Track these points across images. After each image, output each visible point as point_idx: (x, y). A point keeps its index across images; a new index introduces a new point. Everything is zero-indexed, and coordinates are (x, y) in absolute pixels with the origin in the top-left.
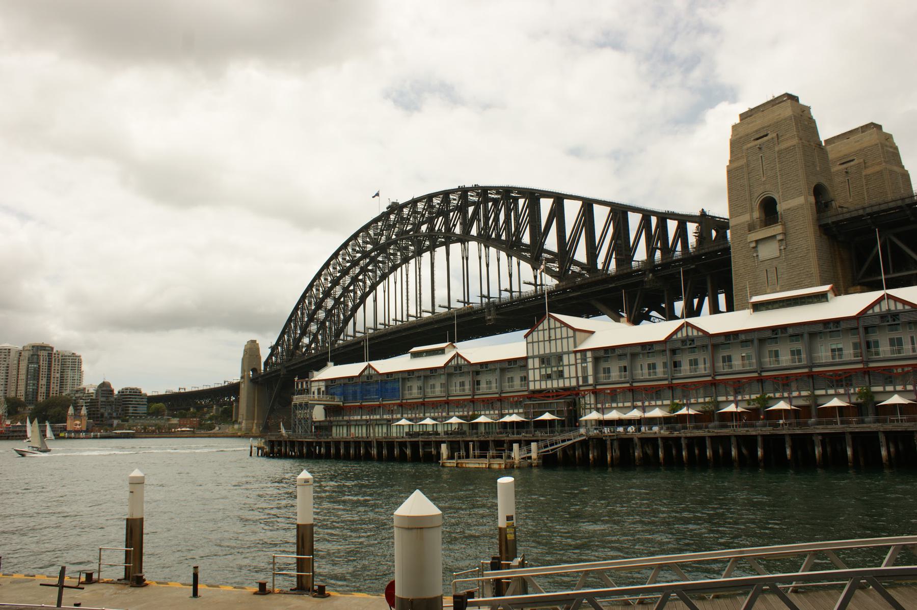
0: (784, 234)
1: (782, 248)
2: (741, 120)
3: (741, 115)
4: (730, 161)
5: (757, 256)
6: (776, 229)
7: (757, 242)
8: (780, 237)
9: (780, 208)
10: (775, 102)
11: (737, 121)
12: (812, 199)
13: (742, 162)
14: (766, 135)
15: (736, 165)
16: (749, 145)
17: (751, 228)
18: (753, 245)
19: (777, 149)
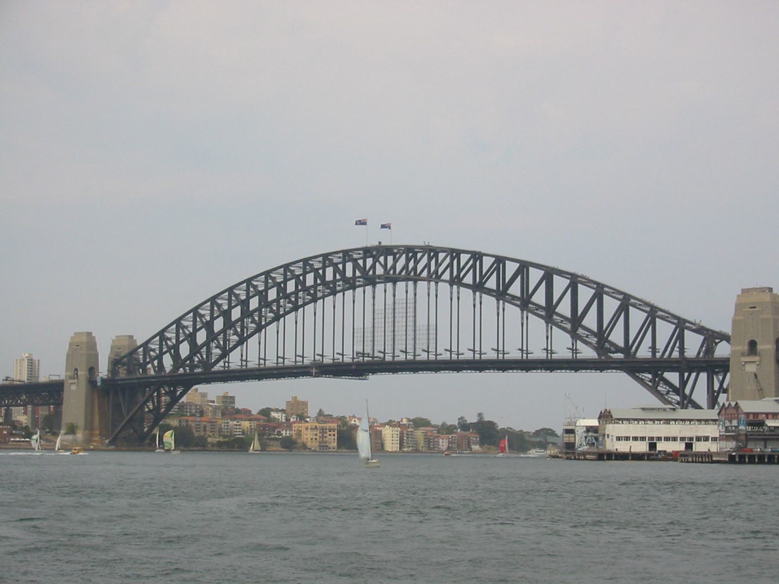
0: (760, 361)
1: (758, 368)
2: (742, 293)
3: (742, 290)
4: (735, 315)
5: (745, 369)
6: (756, 358)
7: (746, 362)
8: (758, 363)
9: (760, 347)
10: (762, 290)
11: (740, 293)
12: (775, 347)
13: (741, 318)
14: (755, 307)
15: (737, 318)
16: (746, 310)
17: (743, 355)
18: (743, 363)
19: (761, 317)
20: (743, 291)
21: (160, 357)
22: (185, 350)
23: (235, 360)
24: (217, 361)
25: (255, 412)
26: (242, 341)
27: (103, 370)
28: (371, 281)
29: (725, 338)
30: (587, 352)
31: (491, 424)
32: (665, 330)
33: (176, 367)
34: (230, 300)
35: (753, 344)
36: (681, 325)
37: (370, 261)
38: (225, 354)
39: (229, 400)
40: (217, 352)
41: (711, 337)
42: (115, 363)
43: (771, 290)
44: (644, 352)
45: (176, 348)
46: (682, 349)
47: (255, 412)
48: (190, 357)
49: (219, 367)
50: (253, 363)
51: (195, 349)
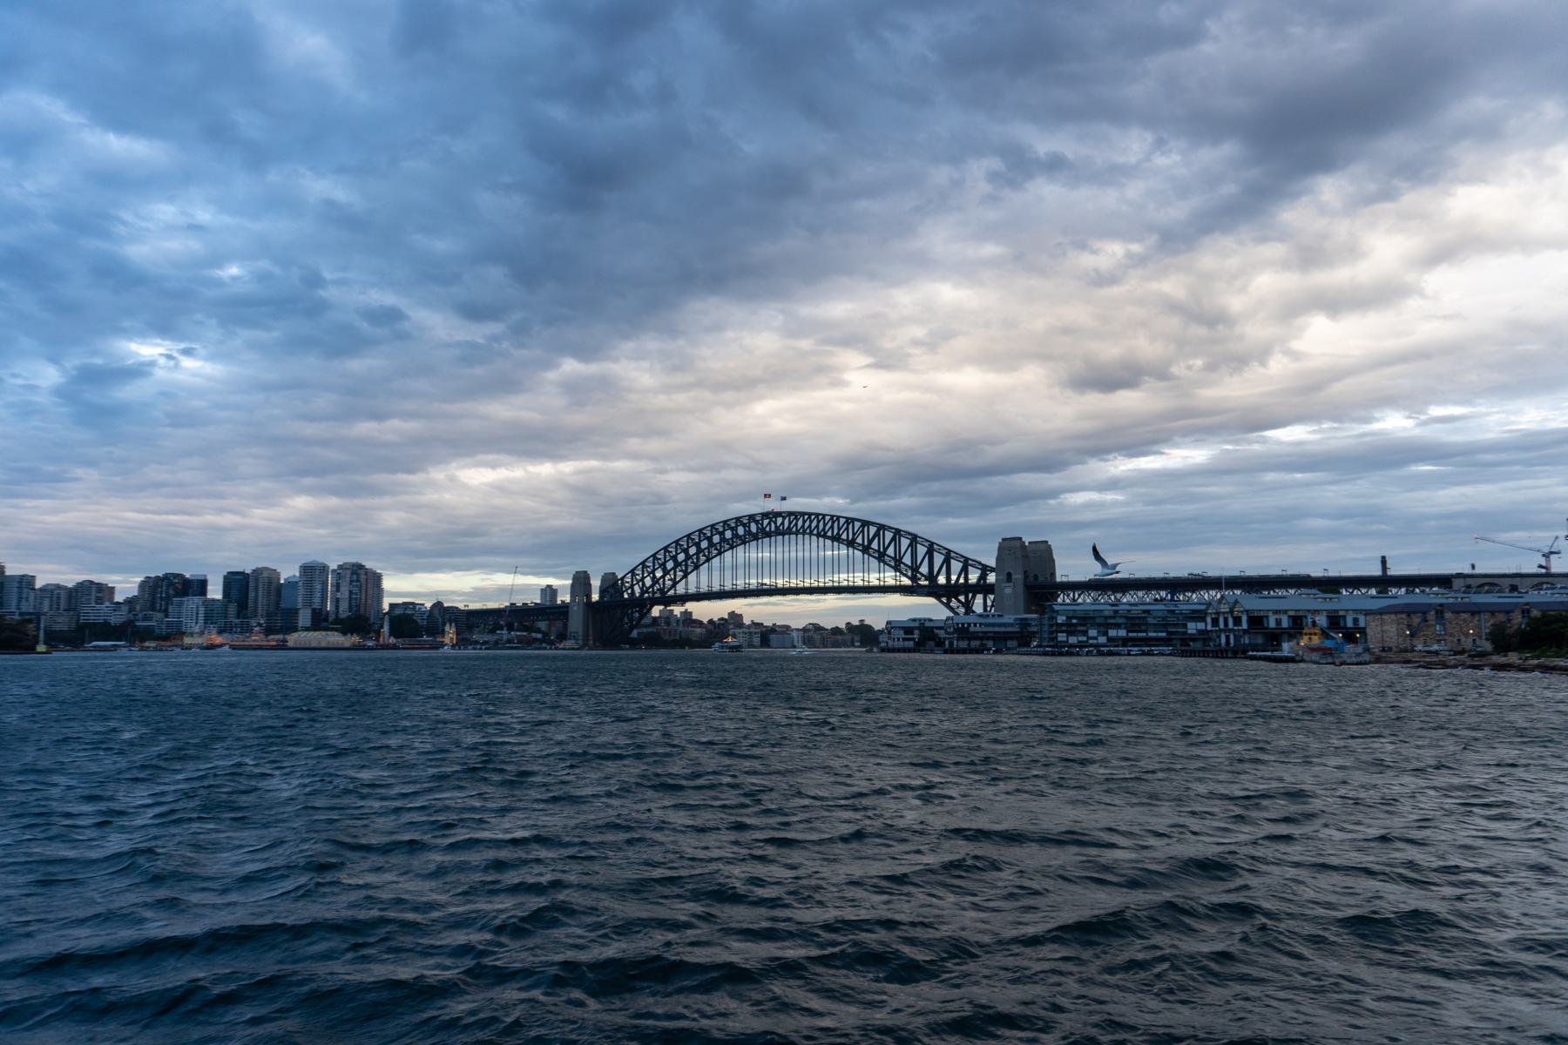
6: (1012, 584)
9: (1013, 577)
20: (1004, 540)
21: (632, 587)
22: (648, 582)
23: (680, 589)
24: (669, 590)
25: (705, 621)
26: (685, 576)
27: (595, 597)
28: (769, 535)
29: (992, 570)
30: (906, 582)
31: (870, 627)
32: (956, 566)
33: (643, 592)
34: (676, 548)
35: (1009, 575)
36: (966, 563)
37: (766, 522)
38: (674, 585)
39: (687, 614)
40: (669, 583)
41: (985, 570)
42: (603, 592)
43: (1021, 539)
44: (942, 580)
45: (643, 579)
46: (966, 578)
47: (705, 621)
48: (652, 586)
49: (671, 592)
50: (692, 590)
51: (655, 581)
